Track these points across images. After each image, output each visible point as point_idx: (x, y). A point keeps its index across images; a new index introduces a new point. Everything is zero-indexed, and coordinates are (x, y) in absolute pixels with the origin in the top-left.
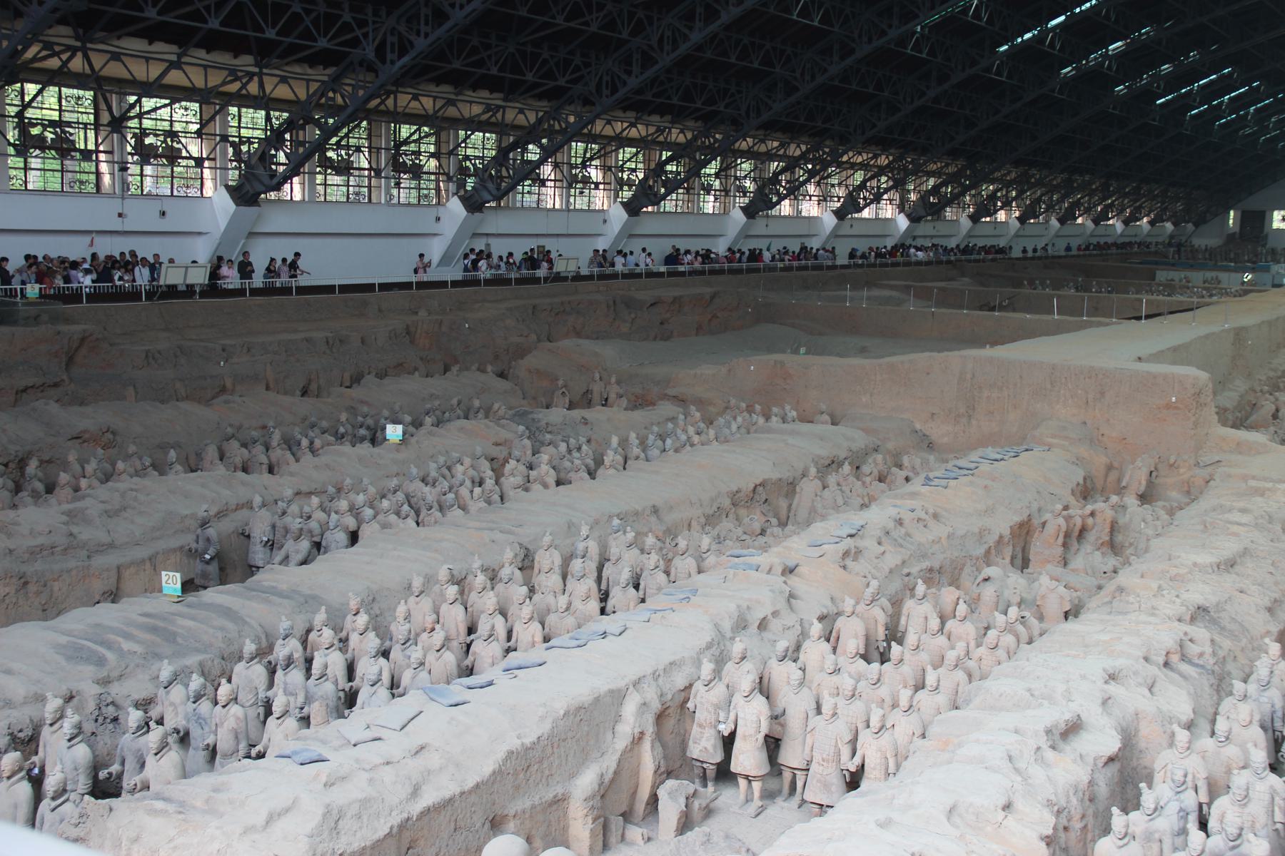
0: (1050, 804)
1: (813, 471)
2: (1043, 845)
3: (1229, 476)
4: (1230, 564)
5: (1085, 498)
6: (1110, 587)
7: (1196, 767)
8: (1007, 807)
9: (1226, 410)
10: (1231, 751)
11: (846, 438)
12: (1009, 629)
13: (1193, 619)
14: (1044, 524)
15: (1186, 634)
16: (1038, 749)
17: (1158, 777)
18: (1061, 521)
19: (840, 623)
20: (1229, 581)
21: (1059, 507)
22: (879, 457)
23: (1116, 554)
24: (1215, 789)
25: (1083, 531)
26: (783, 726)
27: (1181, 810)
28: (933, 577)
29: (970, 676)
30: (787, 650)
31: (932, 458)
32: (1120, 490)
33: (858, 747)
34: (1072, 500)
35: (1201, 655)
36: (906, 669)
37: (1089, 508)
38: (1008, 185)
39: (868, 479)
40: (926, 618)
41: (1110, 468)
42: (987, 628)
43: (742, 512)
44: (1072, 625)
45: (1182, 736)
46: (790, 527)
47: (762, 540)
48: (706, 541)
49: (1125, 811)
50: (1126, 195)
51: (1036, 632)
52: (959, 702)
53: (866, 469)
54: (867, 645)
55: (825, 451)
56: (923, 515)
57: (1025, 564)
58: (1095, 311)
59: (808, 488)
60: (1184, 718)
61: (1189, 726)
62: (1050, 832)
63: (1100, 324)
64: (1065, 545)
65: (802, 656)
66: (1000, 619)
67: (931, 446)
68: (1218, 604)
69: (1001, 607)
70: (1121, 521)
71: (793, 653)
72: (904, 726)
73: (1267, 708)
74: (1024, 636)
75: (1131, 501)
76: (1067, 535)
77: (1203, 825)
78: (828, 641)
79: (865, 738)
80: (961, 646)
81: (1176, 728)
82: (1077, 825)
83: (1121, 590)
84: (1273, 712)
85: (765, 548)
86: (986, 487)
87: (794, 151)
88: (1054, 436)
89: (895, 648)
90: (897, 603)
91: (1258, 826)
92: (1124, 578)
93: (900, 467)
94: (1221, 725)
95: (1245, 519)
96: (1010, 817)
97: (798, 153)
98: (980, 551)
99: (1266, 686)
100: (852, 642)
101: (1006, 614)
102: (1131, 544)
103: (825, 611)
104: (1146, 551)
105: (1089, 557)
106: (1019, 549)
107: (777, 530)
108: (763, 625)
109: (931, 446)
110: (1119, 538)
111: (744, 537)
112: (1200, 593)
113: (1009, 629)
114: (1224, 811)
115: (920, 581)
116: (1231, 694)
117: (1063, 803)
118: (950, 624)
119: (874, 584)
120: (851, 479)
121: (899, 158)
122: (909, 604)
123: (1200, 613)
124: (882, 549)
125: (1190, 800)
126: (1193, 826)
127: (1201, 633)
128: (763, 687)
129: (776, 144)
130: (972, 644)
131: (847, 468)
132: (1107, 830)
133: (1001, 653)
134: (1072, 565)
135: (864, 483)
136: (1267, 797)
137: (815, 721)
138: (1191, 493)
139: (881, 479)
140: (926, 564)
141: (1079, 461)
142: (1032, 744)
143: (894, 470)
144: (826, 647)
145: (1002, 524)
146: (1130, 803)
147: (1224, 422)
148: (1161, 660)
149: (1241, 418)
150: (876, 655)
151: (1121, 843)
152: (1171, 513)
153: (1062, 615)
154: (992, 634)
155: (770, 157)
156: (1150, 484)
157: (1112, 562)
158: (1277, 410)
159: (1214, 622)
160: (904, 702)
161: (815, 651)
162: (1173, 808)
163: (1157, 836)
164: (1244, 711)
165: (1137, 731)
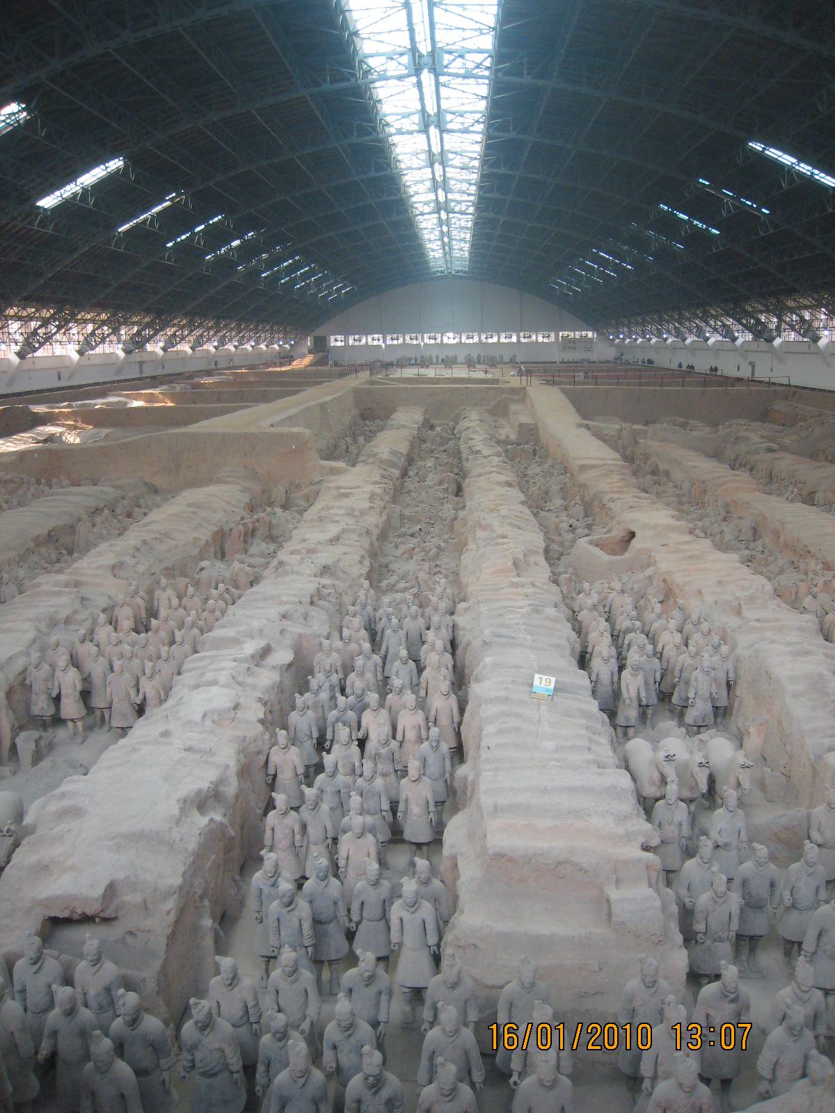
0: (260, 700)
1: (85, 517)
2: (260, 725)
3: (329, 488)
4: (335, 540)
5: (252, 511)
6: (275, 563)
7: (335, 659)
8: (236, 707)
9: (321, 450)
10: (353, 646)
11: (106, 491)
12: (221, 597)
13: (322, 574)
14: (231, 530)
15: (319, 584)
16: (249, 668)
17: (316, 669)
18: (241, 527)
19: (117, 611)
20: (339, 549)
21: (238, 518)
22: (125, 502)
23: (274, 542)
24: (348, 668)
25: (254, 530)
26: (90, 683)
27: (331, 686)
28: (169, 572)
29: (201, 631)
30: (85, 635)
31: (158, 499)
32: (271, 504)
33: (140, 688)
34: (245, 514)
35: (329, 594)
36: (163, 634)
37: (256, 517)
38: (182, 328)
39: (120, 517)
40: (169, 599)
41: (264, 492)
42: (207, 599)
43: (43, 550)
44: (255, 589)
45: (326, 642)
46: (75, 555)
47: (58, 566)
48: (21, 573)
49: (302, 694)
50: (251, 330)
51: (236, 597)
52: (199, 648)
53: (118, 511)
54: (136, 623)
55: (91, 502)
56: (158, 536)
57: (223, 555)
58: (242, 399)
59: (83, 529)
60: (325, 633)
61: (328, 638)
62: (262, 716)
63: (246, 407)
64: (245, 541)
65: (96, 637)
66: (214, 592)
67: (156, 491)
68: (334, 563)
69: (213, 585)
70: (274, 522)
71: (90, 636)
72: (166, 669)
73: (366, 618)
74: (230, 600)
75: (278, 510)
76: (245, 535)
77: (343, 691)
78: (111, 624)
79: (143, 680)
80: (193, 613)
81: (322, 639)
82: (277, 708)
83: (281, 564)
84: (370, 620)
85: (60, 571)
86: (194, 513)
87: (46, 313)
88: (229, 477)
89: (154, 622)
90: (150, 592)
91: (370, 685)
92: (283, 555)
93: (139, 506)
94: (346, 632)
95: (342, 512)
96: (239, 713)
97: (48, 315)
98: (196, 551)
99: (364, 606)
100: (126, 624)
101: (217, 589)
102: (281, 535)
103: (106, 606)
104: (291, 538)
105: (259, 546)
106: (218, 548)
107: (67, 558)
108: (68, 621)
109: (156, 491)
110: (274, 532)
111: (47, 565)
112: (325, 557)
113: (221, 597)
114: (353, 679)
115: (163, 578)
116: (348, 614)
117: (267, 698)
118: (184, 600)
119: (134, 583)
120: (110, 518)
121: (114, 314)
122: (158, 592)
123: (325, 570)
124: (136, 560)
125: (335, 678)
126: (338, 695)
127: (326, 581)
128: (75, 662)
129: (33, 310)
130: (200, 610)
131: (106, 511)
132: (293, 708)
133: (218, 613)
134: (249, 553)
135: (119, 521)
136: (373, 668)
137: (111, 677)
138: (310, 500)
139: (129, 516)
140: (164, 565)
141: (245, 490)
142: (245, 665)
143: (136, 509)
144: (110, 628)
145: (205, 534)
146: (303, 688)
147: (322, 458)
148: (308, 600)
149: (330, 454)
150: (142, 628)
151: (302, 713)
152: (301, 513)
153: (249, 584)
154: (211, 602)
155: (30, 318)
156: (287, 498)
157: (272, 547)
158: (348, 448)
159: (333, 575)
160: (164, 655)
161: (104, 633)
162: (327, 685)
163: (320, 704)
164: (357, 622)
165: (301, 645)
